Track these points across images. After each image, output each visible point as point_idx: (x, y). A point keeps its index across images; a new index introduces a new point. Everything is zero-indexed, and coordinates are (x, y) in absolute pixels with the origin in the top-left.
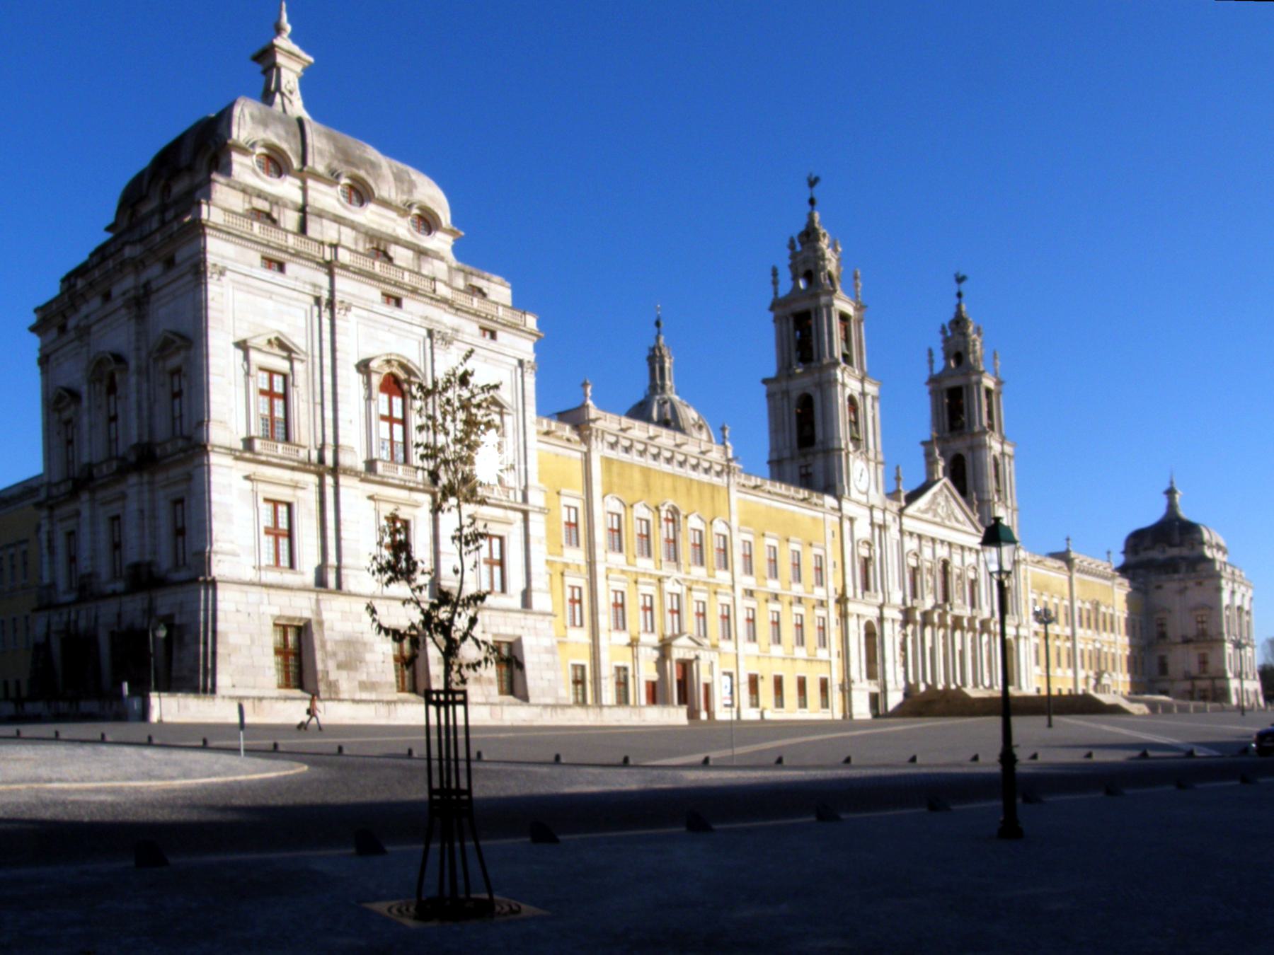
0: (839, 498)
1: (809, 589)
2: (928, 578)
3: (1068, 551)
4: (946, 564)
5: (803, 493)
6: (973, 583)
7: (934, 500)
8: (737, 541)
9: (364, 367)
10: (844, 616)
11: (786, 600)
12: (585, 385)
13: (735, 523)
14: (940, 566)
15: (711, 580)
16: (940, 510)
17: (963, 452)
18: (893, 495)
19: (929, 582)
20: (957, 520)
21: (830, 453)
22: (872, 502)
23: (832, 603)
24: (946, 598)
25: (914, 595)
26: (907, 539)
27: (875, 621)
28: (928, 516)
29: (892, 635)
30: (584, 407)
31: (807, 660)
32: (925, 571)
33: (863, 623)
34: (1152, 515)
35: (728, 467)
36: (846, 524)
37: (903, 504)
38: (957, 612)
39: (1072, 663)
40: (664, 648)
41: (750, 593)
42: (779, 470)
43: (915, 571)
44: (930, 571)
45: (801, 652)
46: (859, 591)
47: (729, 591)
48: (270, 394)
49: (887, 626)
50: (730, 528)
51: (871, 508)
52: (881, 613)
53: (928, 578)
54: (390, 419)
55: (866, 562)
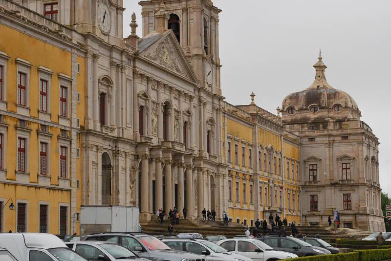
1: (55, 119)
2: (152, 116)
4: (167, 106)
10: (85, 148)
11: (34, 127)
14: (161, 109)
17: (179, 13)
19: (154, 120)
20: (178, 70)
22: (112, 42)
23: (74, 134)
25: (141, 131)
27: (110, 154)
28: (157, 62)
31: (50, 189)
32: (151, 110)
33: (100, 155)
34: (305, 82)
38: (177, 148)
44: (156, 110)
45: (43, 182)
46: (98, 124)
49: (121, 159)
53: (152, 116)
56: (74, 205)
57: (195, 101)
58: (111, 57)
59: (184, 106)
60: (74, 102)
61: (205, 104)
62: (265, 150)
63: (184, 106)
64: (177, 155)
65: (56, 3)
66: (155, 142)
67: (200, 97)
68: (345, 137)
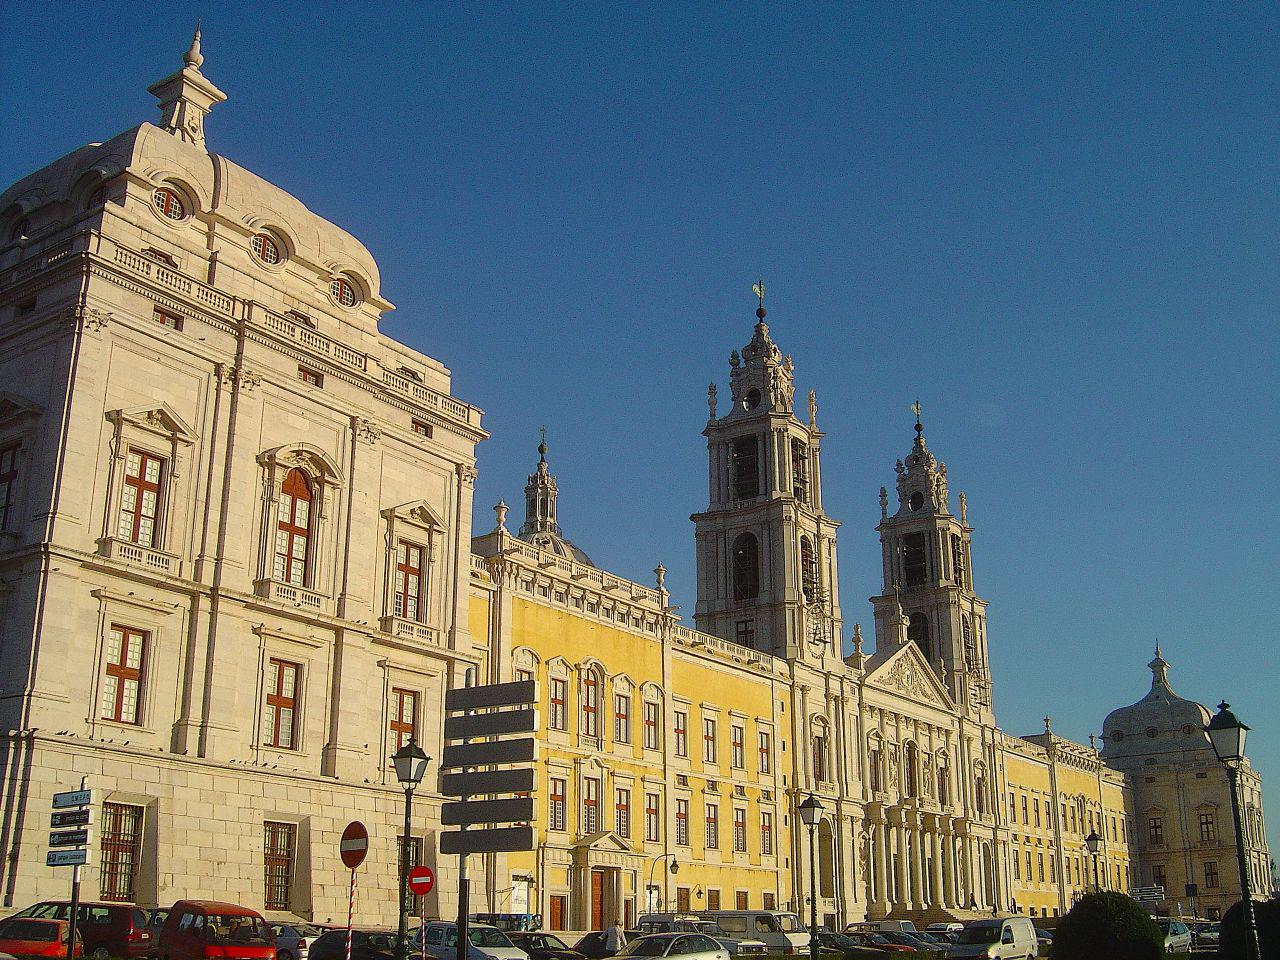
0: (790, 663)
3: (1048, 734)
4: (912, 747)
5: (749, 654)
6: (944, 771)
7: (899, 665)
8: (671, 708)
9: (267, 461)
12: (498, 508)
13: (668, 690)
14: (903, 753)
15: (637, 763)
16: (905, 681)
18: (851, 661)
19: (893, 771)
21: (777, 606)
23: (780, 793)
24: (912, 793)
25: (876, 788)
26: (866, 715)
28: (892, 688)
29: (851, 839)
30: (497, 534)
32: (887, 757)
34: (1135, 689)
35: (664, 617)
36: (798, 694)
37: (864, 672)
38: (927, 809)
39: (1057, 878)
40: (579, 852)
41: (683, 780)
42: (707, 621)
43: (877, 755)
44: (895, 758)
46: (812, 781)
47: (660, 778)
48: (139, 483)
49: (846, 826)
50: (663, 696)
51: (827, 676)
52: (839, 810)
54: (290, 528)
55: (820, 743)
56: (782, 891)
57: (954, 738)
58: (827, 684)
59: (939, 742)
60: (779, 751)
61: (969, 740)
62: (1072, 800)
63: (939, 742)
64: (928, 818)
65: (752, 621)
66: (893, 801)
67: (961, 731)
68: (1201, 776)
